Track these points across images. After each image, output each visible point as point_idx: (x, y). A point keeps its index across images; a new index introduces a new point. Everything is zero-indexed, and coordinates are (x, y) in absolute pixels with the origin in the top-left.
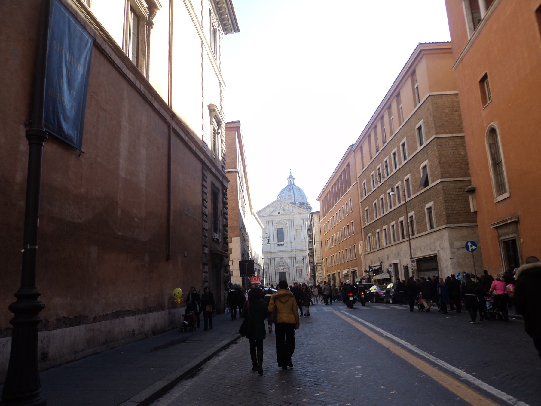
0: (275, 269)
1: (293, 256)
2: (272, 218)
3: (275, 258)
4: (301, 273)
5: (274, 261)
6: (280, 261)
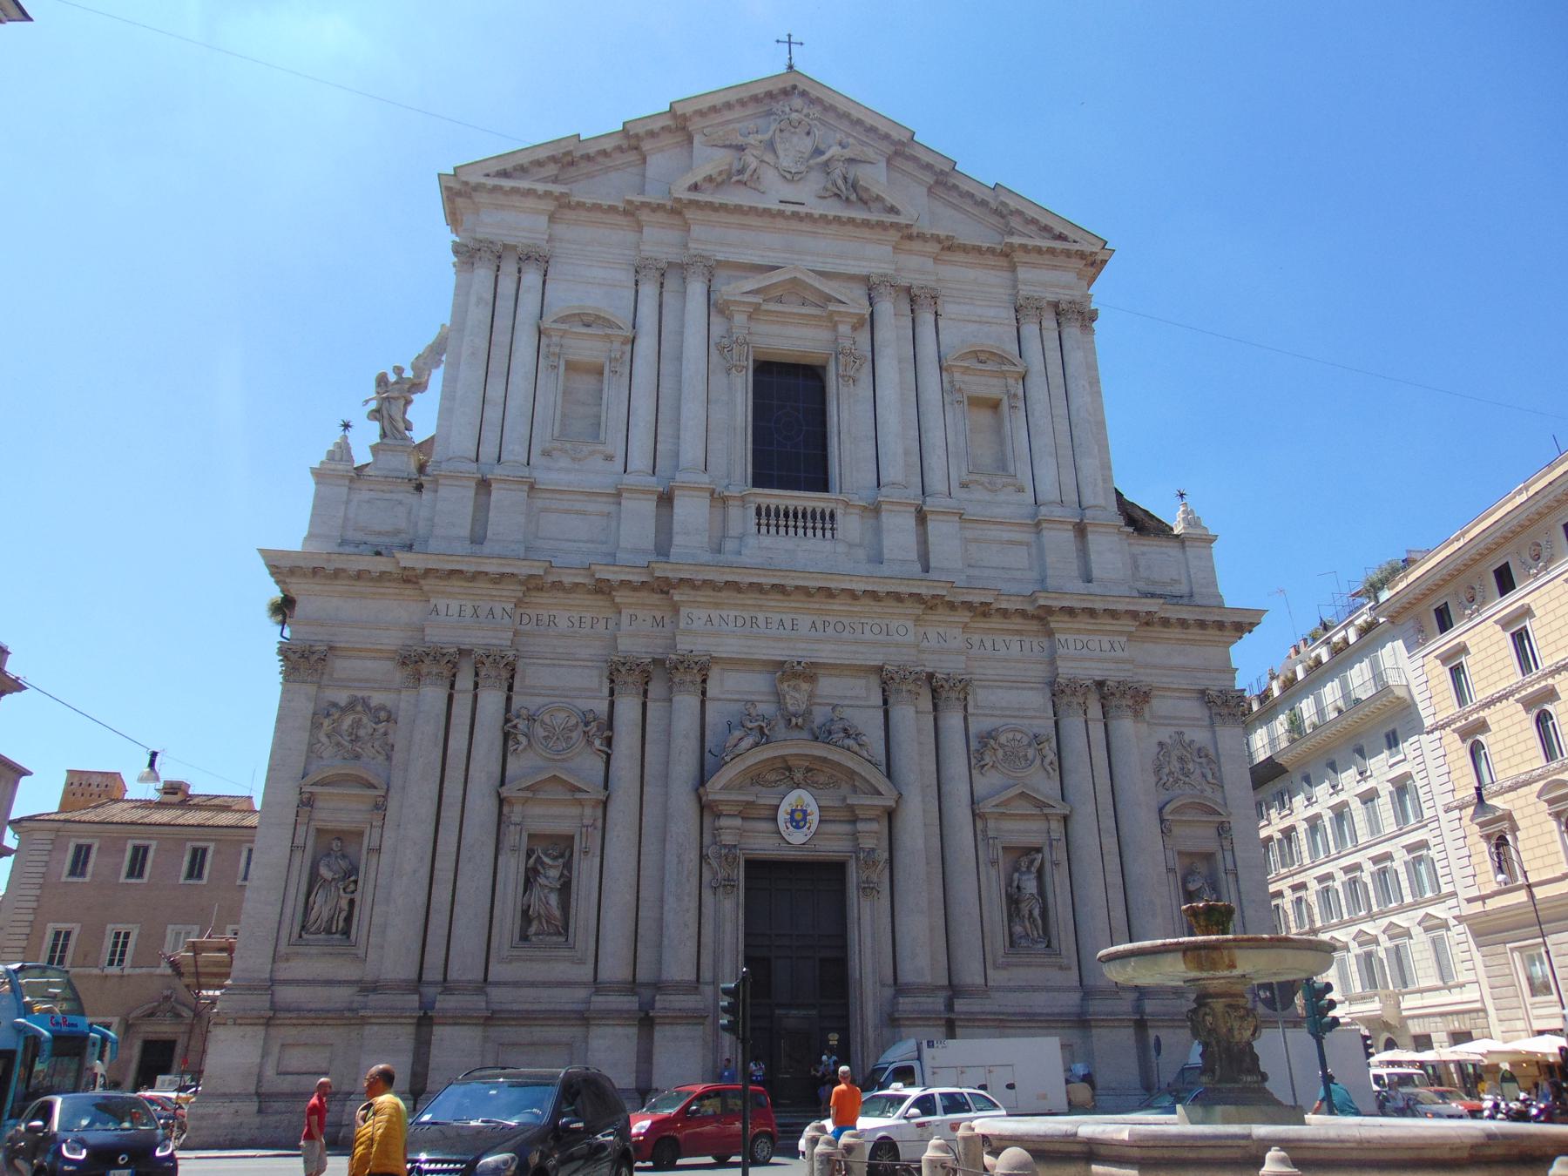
0: (705, 808)
1: (946, 665)
2: (711, 239)
3: (714, 674)
4: (1030, 886)
5: (695, 701)
6: (766, 708)
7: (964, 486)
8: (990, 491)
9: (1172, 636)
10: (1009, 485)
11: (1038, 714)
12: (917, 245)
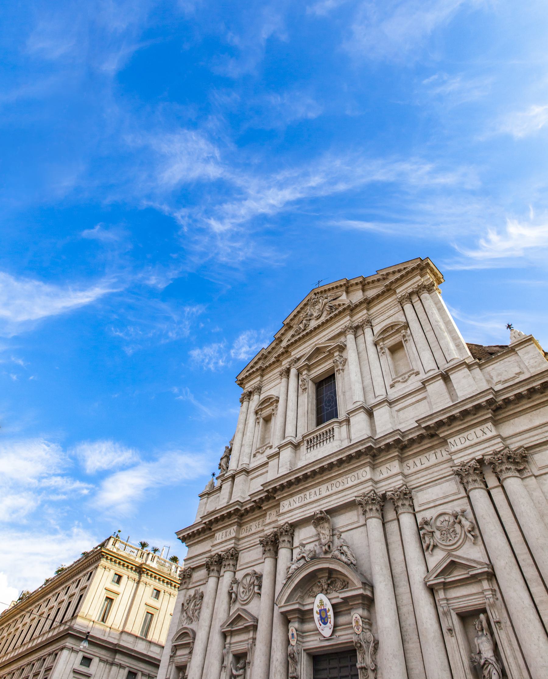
7: (392, 386)
8: (405, 382)
9: (525, 407)
10: (411, 374)
11: (456, 497)
12: (358, 309)
